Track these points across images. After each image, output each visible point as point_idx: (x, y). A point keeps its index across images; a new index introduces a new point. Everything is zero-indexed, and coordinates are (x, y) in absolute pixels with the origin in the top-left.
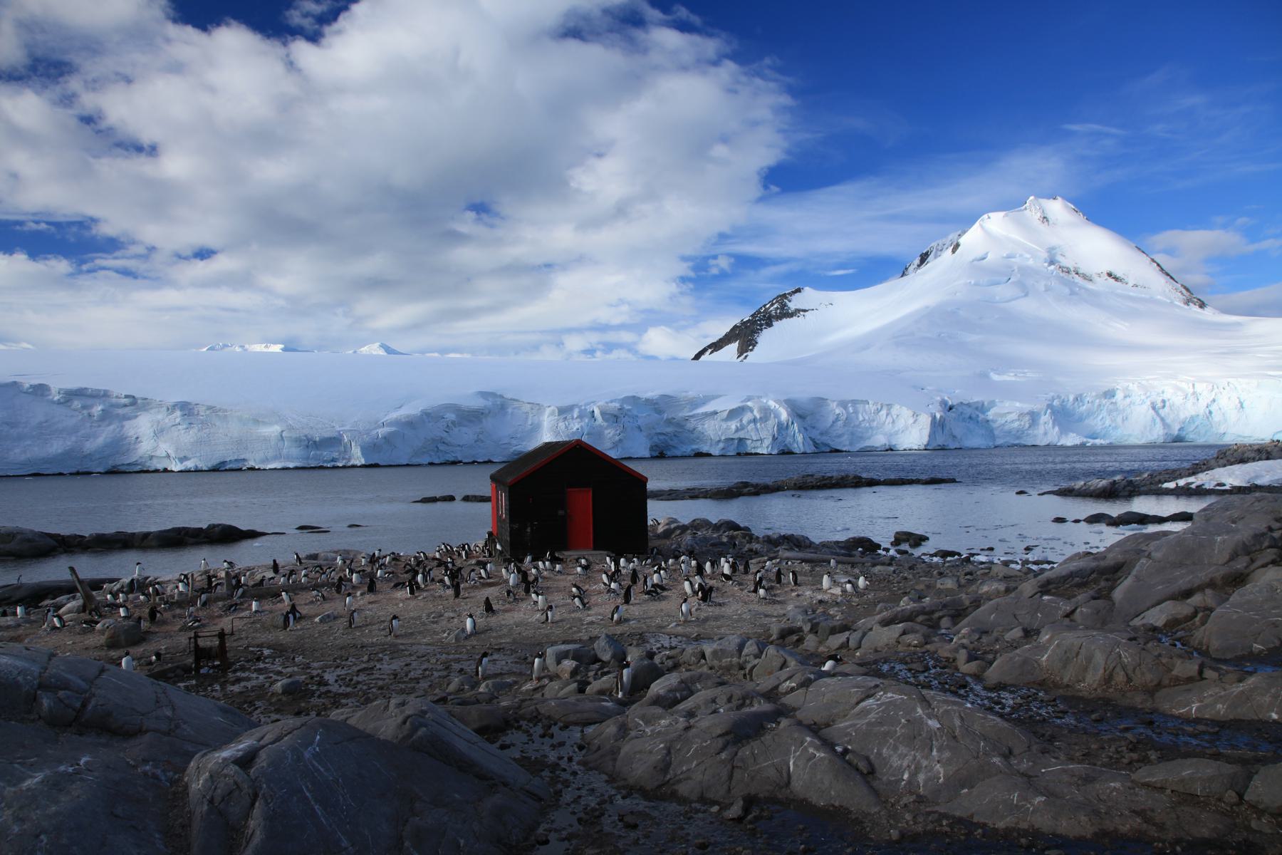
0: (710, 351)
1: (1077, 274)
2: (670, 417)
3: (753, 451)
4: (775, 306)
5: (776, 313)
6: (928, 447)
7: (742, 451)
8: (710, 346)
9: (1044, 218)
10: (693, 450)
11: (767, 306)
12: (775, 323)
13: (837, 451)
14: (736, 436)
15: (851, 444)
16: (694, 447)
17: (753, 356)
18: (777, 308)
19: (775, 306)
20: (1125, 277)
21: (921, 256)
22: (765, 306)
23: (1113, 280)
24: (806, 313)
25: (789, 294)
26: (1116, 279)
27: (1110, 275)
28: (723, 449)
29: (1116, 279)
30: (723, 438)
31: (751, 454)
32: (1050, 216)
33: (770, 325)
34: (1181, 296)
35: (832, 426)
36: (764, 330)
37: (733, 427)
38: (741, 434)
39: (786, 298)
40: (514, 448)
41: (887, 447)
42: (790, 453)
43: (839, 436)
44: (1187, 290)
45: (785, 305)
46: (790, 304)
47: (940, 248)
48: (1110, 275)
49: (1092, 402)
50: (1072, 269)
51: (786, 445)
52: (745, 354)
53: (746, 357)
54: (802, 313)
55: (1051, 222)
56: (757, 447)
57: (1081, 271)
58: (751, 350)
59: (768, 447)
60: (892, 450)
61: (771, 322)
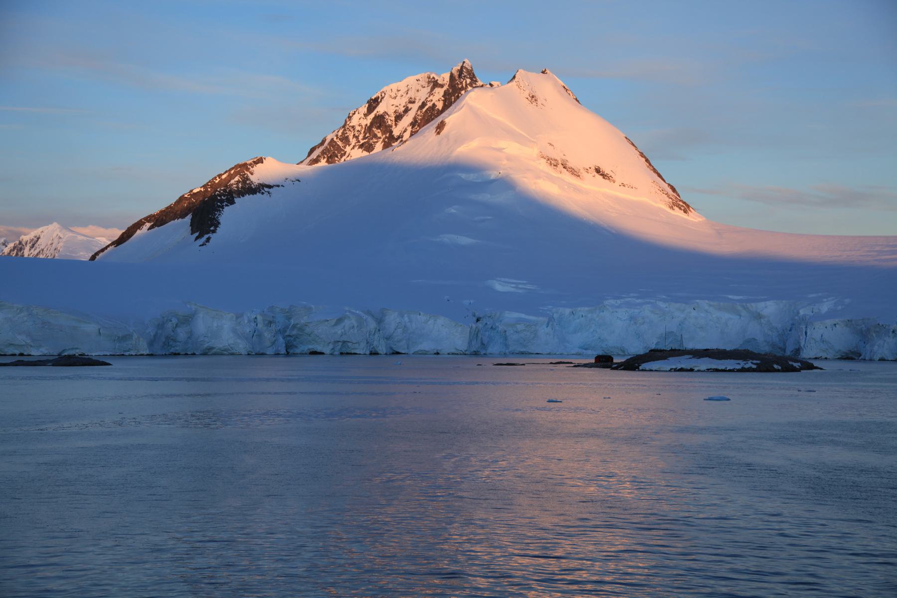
0: (148, 225)
1: (564, 167)
2: (296, 323)
3: (353, 351)
4: (237, 178)
5: (238, 187)
6: (467, 353)
7: (344, 350)
8: (148, 219)
9: (533, 97)
10: (309, 349)
11: (224, 177)
12: (236, 200)
13: (398, 353)
15: (408, 348)
16: (310, 347)
17: (218, 237)
18: (238, 182)
19: (237, 178)
20: (611, 174)
21: (368, 102)
22: (220, 176)
23: (601, 177)
24: (271, 190)
25: (250, 164)
26: (604, 176)
27: (598, 171)
28: (333, 349)
29: (604, 176)
30: (333, 341)
32: (538, 95)
33: (231, 202)
34: (667, 199)
35: (393, 332)
36: (226, 208)
37: (339, 332)
38: (345, 338)
39: (248, 169)
40: (207, 345)
41: (435, 352)
42: (376, 354)
43: (400, 341)
44: (674, 190)
45: (248, 179)
46: (252, 178)
47: (393, 95)
48: (598, 171)
49: (585, 316)
50: (560, 162)
52: (206, 236)
53: (208, 240)
54: (266, 189)
55: (539, 102)
56: (356, 349)
57: (569, 165)
58: (214, 232)
59: (363, 349)
60: (438, 354)
61: (233, 198)
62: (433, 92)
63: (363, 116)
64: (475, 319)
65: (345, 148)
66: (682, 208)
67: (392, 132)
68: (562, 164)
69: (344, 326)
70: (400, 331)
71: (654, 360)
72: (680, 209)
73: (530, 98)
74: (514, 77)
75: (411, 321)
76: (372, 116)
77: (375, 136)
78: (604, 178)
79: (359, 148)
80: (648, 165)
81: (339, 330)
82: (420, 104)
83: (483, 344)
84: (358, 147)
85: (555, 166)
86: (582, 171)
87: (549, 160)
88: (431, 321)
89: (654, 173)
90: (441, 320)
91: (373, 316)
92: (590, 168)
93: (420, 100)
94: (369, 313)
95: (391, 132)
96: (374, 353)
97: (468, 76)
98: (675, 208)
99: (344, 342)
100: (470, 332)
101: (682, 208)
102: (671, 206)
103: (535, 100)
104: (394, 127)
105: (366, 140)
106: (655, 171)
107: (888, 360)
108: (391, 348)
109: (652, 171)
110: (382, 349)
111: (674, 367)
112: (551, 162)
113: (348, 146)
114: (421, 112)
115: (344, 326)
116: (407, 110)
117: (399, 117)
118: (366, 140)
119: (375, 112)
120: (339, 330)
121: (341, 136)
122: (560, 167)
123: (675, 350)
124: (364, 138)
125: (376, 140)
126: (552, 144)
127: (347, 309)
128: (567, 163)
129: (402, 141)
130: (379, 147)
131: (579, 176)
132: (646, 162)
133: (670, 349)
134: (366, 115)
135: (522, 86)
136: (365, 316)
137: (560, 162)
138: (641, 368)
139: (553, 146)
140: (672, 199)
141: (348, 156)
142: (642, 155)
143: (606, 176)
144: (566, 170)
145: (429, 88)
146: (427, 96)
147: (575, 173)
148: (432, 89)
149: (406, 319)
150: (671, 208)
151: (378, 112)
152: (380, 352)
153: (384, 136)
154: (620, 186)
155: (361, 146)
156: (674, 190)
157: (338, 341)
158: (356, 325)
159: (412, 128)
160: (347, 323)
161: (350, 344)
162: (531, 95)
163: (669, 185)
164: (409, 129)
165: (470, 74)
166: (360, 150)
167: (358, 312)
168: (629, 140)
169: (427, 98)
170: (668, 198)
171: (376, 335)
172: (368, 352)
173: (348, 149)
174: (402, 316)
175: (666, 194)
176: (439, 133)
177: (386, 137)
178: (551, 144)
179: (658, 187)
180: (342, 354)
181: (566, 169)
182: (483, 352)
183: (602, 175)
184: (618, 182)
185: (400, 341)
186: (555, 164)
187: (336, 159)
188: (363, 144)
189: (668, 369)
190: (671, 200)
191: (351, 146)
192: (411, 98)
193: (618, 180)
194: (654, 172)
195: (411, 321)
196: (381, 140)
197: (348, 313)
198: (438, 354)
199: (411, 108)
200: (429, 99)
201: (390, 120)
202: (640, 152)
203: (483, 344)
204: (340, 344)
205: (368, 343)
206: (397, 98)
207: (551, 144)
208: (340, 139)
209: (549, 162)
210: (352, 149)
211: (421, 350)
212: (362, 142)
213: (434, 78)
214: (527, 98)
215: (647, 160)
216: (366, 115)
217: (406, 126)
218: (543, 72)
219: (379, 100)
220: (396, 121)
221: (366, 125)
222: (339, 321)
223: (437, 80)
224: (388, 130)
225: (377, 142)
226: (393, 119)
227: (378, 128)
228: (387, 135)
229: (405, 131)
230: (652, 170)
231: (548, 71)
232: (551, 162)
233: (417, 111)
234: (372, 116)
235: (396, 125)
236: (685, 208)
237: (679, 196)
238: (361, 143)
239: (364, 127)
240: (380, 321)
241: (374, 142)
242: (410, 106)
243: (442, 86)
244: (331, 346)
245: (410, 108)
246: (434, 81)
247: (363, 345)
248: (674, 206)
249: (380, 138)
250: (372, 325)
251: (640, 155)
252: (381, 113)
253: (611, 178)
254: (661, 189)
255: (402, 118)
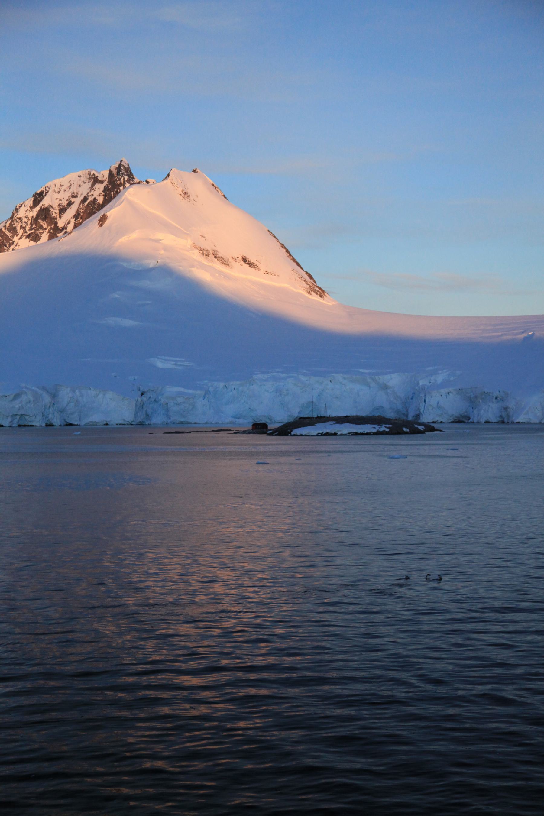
1: (215, 257)
3: (30, 424)
6: (133, 423)
7: (22, 423)
9: (186, 193)
13: (71, 424)
14: (19, 413)
15: (80, 420)
20: (256, 263)
21: (34, 196)
23: (248, 266)
27: (245, 260)
28: (11, 422)
29: (250, 264)
30: (11, 414)
31: (28, 426)
32: (190, 191)
35: (67, 405)
37: (17, 406)
38: (22, 412)
41: (105, 423)
42: (52, 425)
43: (72, 414)
44: (311, 277)
47: (57, 190)
48: (245, 260)
50: (211, 252)
51: (49, 420)
55: (191, 198)
56: (33, 421)
57: (219, 255)
59: (39, 421)
60: (107, 424)
62: (94, 188)
63: (29, 208)
64: (140, 393)
65: (13, 238)
66: (319, 293)
67: (57, 224)
68: (213, 254)
69: (21, 401)
70: (72, 404)
71: (304, 426)
72: (317, 294)
73: (183, 195)
74: (168, 175)
75: (82, 396)
76: (38, 208)
77: (41, 227)
78: (250, 266)
79: (26, 238)
80: (288, 255)
81: (16, 404)
82: (82, 198)
83: (147, 415)
84: (25, 237)
85: (207, 255)
86: (231, 260)
87: (201, 250)
88: (101, 396)
89: (293, 262)
90: (110, 395)
91: (47, 392)
92: (238, 258)
93: (82, 194)
94: (44, 389)
95: (56, 224)
96: (49, 425)
97: (126, 174)
98: (313, 293)
99: (22, 415)
100: (136, 405)
101: (319, 293)
102: (308, 291)
103: (188, 196)
104: (58, 219)
105: (33, 231)
106: (294, 260)
107: (492, 423)
108: (65, 420)
109: (292, 261)
110: (57, 421)
111: (321, 432)
112: (203, 252)
113: (15, 236)
114: (83, 206)
115: (21, 401)
116: (70, 204)
117: (62, 210)
118: (33, 231)
119: (40, 205)
120: (16, 404)
121: (9, 227)
122: (211, 256)
123: (321, 417)
124: (31, 229)
125: (42, 231)
126: (204, 235)
127: (24, 385)
128: (218, 253)
129: (66, 231)
130: (45, 237)
131: (228, 265)
132: (286, 253)
133: (317, 416)
134: (32, 208)
135: (176, 184)
136: (41, 392)
137: (211, 252)
138: (293, 433)
139: (205, 238)
140: (309, 285)
141: (16, 245)
142: (283, 246)
143: (252, 265)
144: (216, 259)
145: (90, 184)
146: (89, 191)
147: (225, 262)
148: (93, 185)
149: (78, 393)
150: (309, 293)
151: (43, 205)
152: (54, 424)
153: (49, 227)
154: (264, 273)
155: (28, 236)
156: (311, 277)
157: (16, 415)
158: (32, 399)
159: (75, 220)
160: (24, 398)
161: (27, 417)
162: (184, 192)
163: (307, 272)
164: (73, 221)
165: (127, 172)
166: (28, 240)
167: (33, 388)
168: (272, 233)
169: (88, 193)
170: (306, 285)
171: (51, 410)
172: (44, 424)
173: (16, 239)
174: (74, 391)
175: (304, 281)
176: (101, 225)
177: (51, 228)
178: (202, 236)
179: (297, 274)
180: (19, 426)
181: (216, 258)
182: (147, 423)
183: (248, 264)
184: (262, 271)
185: (72, 414)
186: (207, 254)
187: (5, 248)
188: (30, 234)
189: (316, 433)
190: (308, 286)
191: (19, 236)
192: (73, 193)
193: (263, 269)
194: (293, 261)
195: (82, 396)
196: (47, 231)
197: (24, 389)
198: (107, 424)
199: (74, 202)
200: (90, 194)
201: (55, 212)
202: (281, 244)
203: (147, 415)
204: (18, 417)
205: (43, 416)
206: (60, 192)
207: (202, 236)
208: (8, 230)
209: (201, 252)
210: (19, 239)
211: (92, 422)
212: (29, 232)
213: (94, 174)
214: (181, 195)
215: (287, 251)
216: (32, 208)
217: (69, 218)
218: (194, 171)
219: (44, 194)
220: (60, 213)
221: (33, 217)
222: (17, 396)
223: (98, 177)
224: (53, 221)
225: (43, 233)
226: (57, 211)
227: (44, 219)
228: (53, 226)
229: (69, 223)
230: (292, 259)
231: (198, 170)
232: (203, 252)
233: (80, 205)
234: (38, 208)
235: (60, 217)
236: (321, 293)
237: (315, 283)
238: (28, 234)
239: (30, 219)
240: (54, 396)
241: (40, 233)
242: (73, 200)
243: (102, 182)
244: (10, 419)
245: (72, 202)
246: (94, 178)
247: (39, 417)
248: (311, 291)
249: (46, 229)
250: (47, 399)
251: (281, 246)
252: (46, 206)
253: (256, 266)
254: (299, 276)
255: (65, 211)
